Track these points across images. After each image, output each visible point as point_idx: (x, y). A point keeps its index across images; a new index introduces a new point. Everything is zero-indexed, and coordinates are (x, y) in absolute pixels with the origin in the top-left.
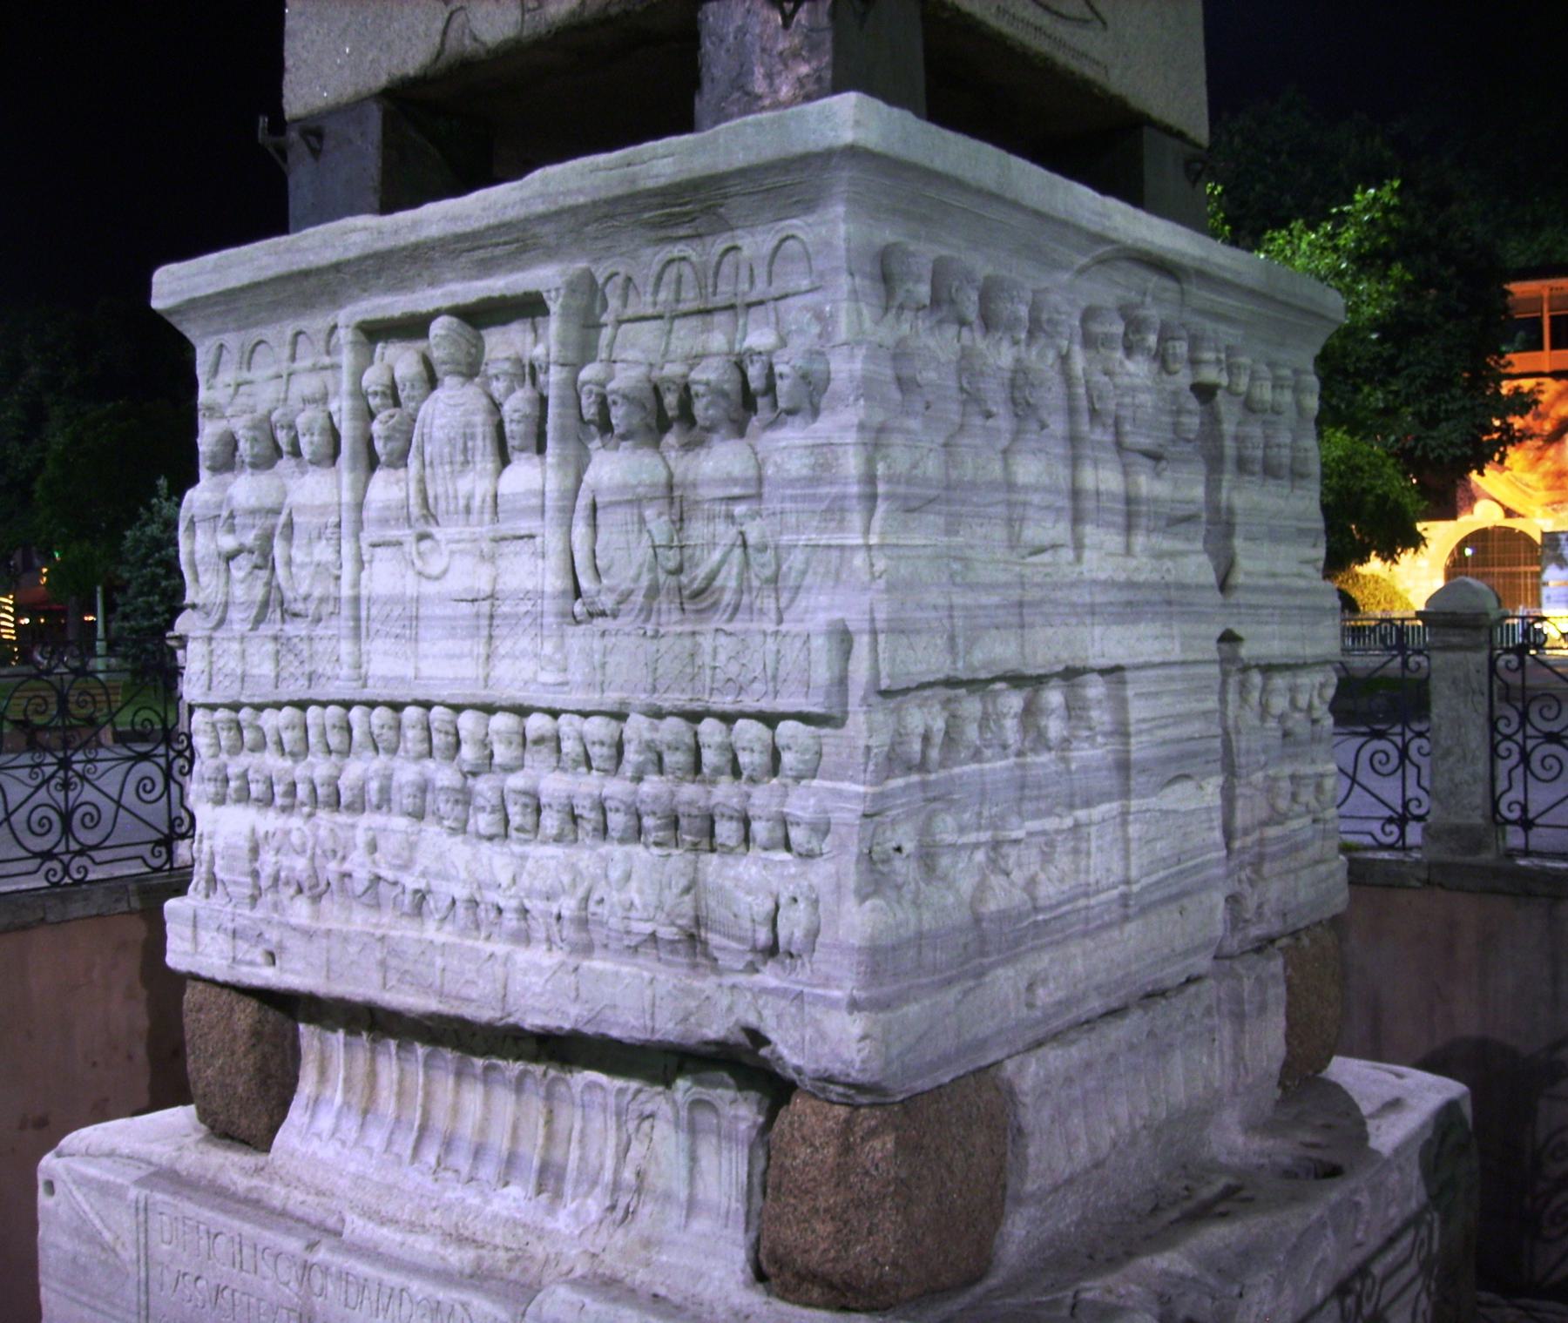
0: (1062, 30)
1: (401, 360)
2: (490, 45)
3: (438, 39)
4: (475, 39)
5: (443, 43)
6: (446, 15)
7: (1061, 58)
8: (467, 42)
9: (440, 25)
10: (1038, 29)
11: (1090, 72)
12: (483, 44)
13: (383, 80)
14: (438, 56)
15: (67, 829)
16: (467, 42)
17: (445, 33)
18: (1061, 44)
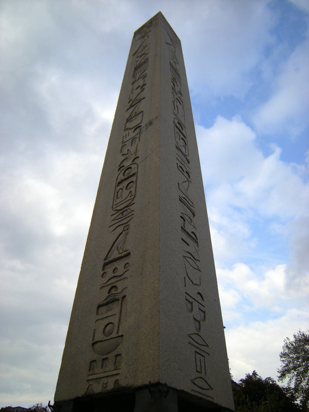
0: (204, 392)
2: (96, 393)
3: (86, 390)
4: (93, 391)
5: (87, 391)
6: (88, 386)
7: (204, 397)
8: (91, 391)
9: (87, 387)
10: (199, 393)
11: (210, 399)
12: (95, 393)
13: (74, 397)
14: (86, 393)
16: (91, 391)
17: (87, 389)
18: (204, 395)
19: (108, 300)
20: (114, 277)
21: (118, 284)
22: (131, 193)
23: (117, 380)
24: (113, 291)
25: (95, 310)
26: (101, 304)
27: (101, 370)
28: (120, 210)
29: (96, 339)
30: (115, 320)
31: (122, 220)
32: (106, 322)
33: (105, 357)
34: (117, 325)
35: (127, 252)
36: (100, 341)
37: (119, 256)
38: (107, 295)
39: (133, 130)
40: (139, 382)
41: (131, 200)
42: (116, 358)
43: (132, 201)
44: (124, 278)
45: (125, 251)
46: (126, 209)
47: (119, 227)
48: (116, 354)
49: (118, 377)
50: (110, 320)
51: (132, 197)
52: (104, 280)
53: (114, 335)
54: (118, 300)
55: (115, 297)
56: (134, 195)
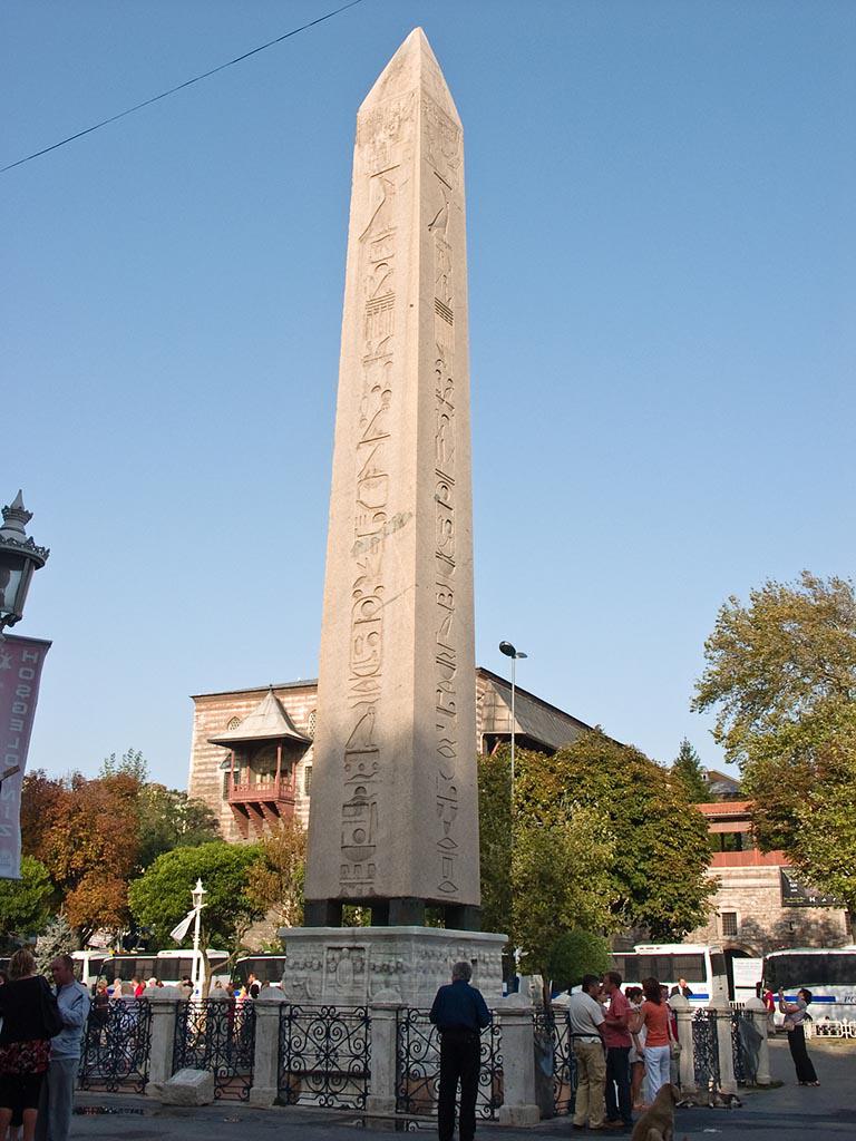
1: (337, 955)
13: (327, 897)
15: (328, 1029)
30: (366, 828)
32: (355, 826)
35: (374, 748)
38: (353, 795)
41: (375, 668)
46: (369, 678)
49: (372, 886)
53: (365, 843)
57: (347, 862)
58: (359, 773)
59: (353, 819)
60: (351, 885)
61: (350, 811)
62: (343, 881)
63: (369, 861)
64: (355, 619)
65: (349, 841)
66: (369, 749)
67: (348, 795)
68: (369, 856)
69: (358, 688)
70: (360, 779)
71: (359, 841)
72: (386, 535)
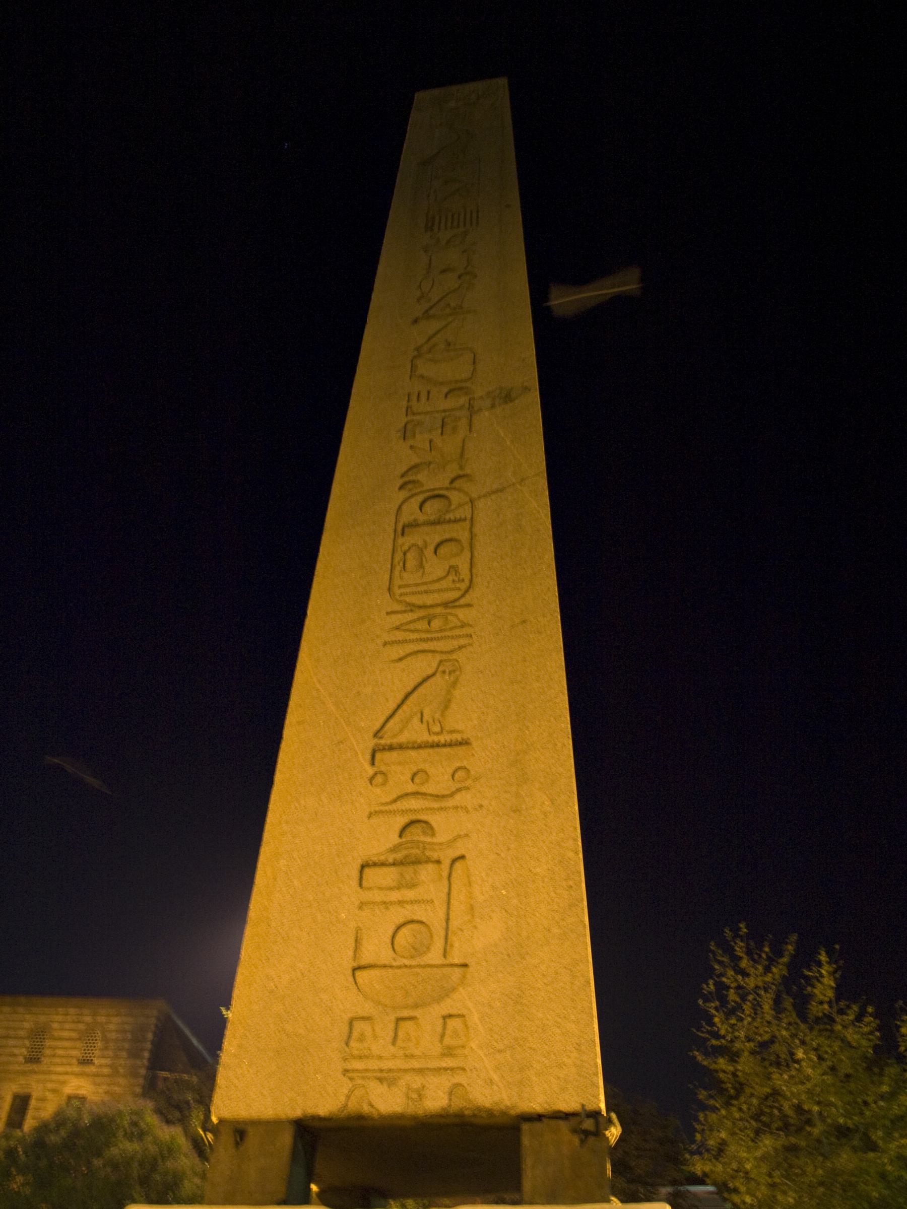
13: (298, 1113)
19: (399, 856)
20: (416, 794)
21: (435, 820)
22: (457, 572)
23: (458, 1085)
24: (416, 834)
25: (355, 874)
26: (375, 859)
27: (393, 1049)
28: (420, 607)
29: (367, 957)
30: (434, 916)
31: (432, 639)
32: (398, 915)
33: (406, 1013)
34: (442, 933)
35: (458, 737)
36: (385, 966)
37: (426, 737)
38: (394, 838)
39: (445, 390)
40: (536, 1104)
41: (457, 594)
42: (445, 1024)
43: (463, 596)
44: (456, 807)
45: (451, 732)
47: (421, 656)
48: (445, 1012)
49: (459, 1078)
50: (419, 913)
51: (464, 586)
52: (382, 795)
53: (434, 956)
54: (438, 862)
55: (428, 853)
56: (467, 582)
57: (367, 1009)
58: (411, 788)
59: (395, 896)
60: (386, 1078)
61: (388, 876)
62: (358, 1065)
63: (446, 1007)
64: (405, 518)
65: (375, 949)
66: (442, 739)
67: (383, 838)
68: (447, 992)
69: (412, 627)
70: (414, 803)
71: (418, 950)
72: (472, 410)
